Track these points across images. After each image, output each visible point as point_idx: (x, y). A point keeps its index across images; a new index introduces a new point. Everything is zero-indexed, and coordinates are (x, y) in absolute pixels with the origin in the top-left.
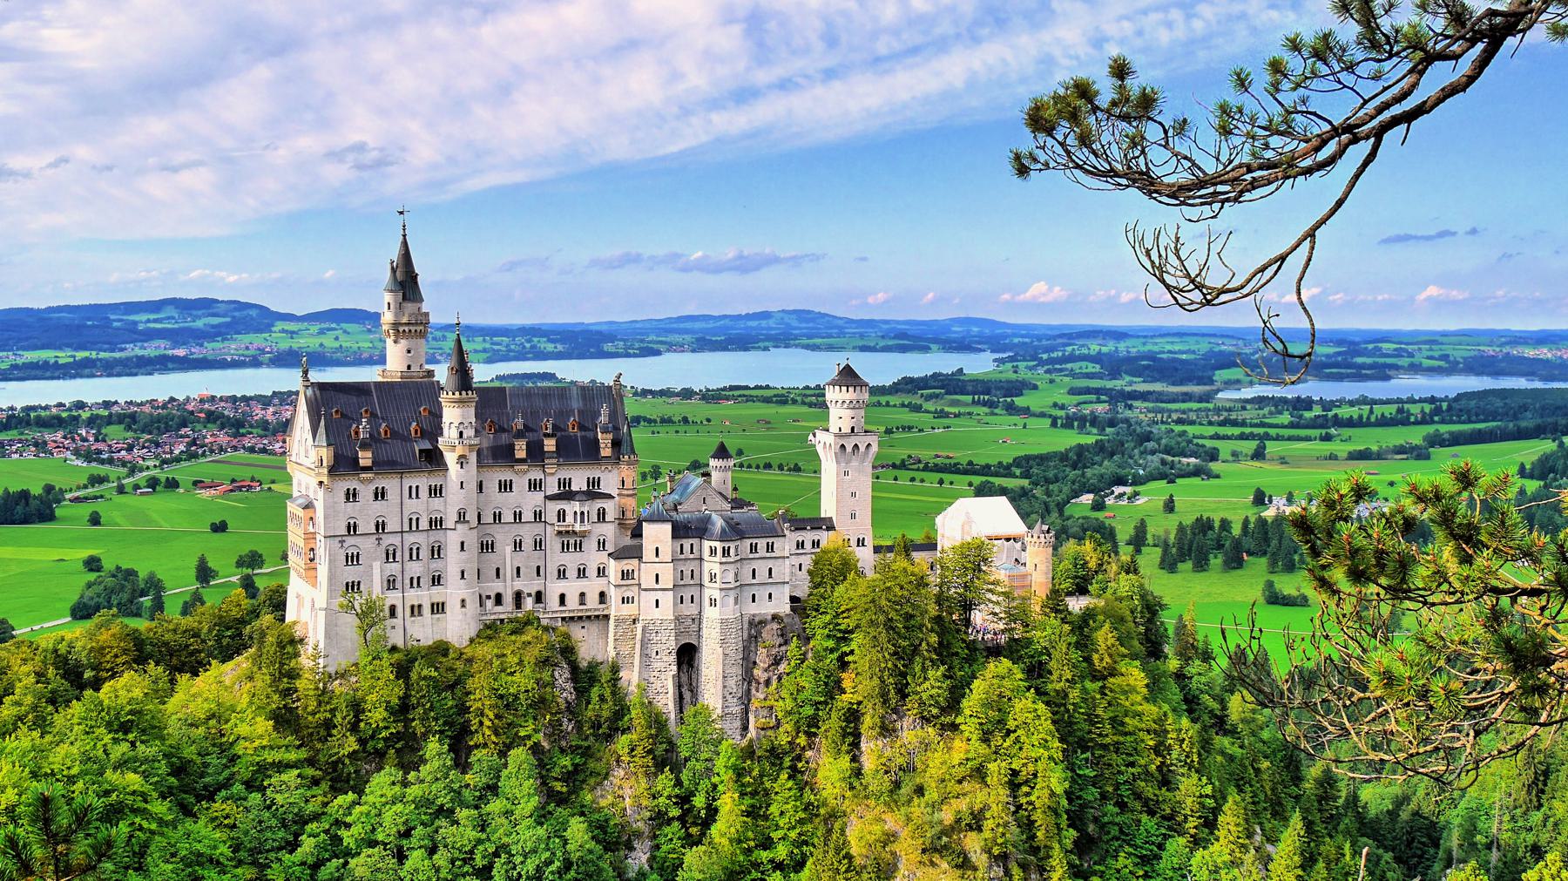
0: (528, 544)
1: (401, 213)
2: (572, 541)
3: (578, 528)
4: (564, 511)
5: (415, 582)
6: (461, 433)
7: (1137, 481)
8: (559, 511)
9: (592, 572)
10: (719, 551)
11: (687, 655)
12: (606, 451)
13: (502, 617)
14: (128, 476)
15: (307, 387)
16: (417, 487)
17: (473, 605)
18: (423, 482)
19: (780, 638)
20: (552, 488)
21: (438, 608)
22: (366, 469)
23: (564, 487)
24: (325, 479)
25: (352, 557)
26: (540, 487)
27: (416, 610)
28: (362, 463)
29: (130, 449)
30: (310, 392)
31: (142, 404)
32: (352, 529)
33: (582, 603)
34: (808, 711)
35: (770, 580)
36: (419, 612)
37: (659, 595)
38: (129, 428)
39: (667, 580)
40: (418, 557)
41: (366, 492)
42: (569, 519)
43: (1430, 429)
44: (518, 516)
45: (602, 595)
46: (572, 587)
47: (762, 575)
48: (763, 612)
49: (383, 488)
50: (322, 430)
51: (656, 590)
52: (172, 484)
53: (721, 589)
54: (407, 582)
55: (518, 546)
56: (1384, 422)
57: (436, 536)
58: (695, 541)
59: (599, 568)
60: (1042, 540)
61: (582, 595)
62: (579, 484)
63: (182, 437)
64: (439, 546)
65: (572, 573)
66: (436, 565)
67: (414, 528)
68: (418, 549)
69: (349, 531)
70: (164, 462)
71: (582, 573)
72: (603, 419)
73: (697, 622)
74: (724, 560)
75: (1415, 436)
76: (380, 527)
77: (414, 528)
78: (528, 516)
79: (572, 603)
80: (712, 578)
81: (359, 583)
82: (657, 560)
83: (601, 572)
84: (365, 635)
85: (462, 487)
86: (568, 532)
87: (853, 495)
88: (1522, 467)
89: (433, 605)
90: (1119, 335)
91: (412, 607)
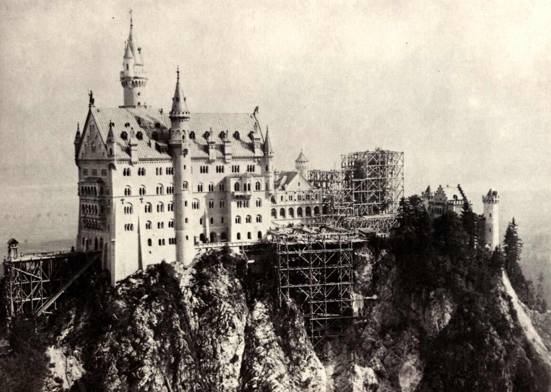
2: (243, 202)
8: (235, 184)
16: (161, 169)
17: (191, 239)
25: (128, 209)
27: (161, 242)
32: (128, 192)
41: (134, 170)
44: (211, 188)
49: (143, 169)
65: (243, 220)
68: (161, 206)
69: (126, 194)
76: (142, 191)
79: (244, 237)
89: (170, 239)
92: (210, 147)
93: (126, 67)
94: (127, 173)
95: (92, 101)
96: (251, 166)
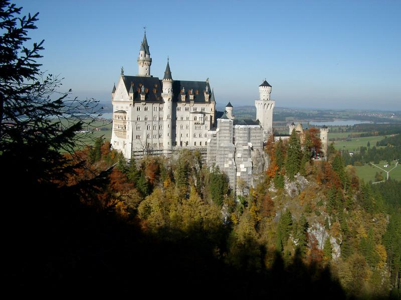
0: (184, 127)
1: (145, 28)
3: (200, 122)
5: (154, 137)
9: (203, 135)
12: (207, 100)
15: (123, 77)
18: (157, 105)
21: (161, 144)
22: (143, 101)
24: (132, 103)
28: (142, 99)
33: (200, 145)
41: (142, 109)
42: (198, 119)
43: (350, 134)
46: (198, 140)
50: (131, 89)
55: (181, 127)
56: (335, 132)
61: (201, 143)
62: (199, 110)
65: (197, 136)
75: (346, 135)
78: (185, 119)
79: (198, 144)
87: (267, 118)
88: (378, 143)
93: (141, 55)
94: (138, 109)
95: (123, 72)
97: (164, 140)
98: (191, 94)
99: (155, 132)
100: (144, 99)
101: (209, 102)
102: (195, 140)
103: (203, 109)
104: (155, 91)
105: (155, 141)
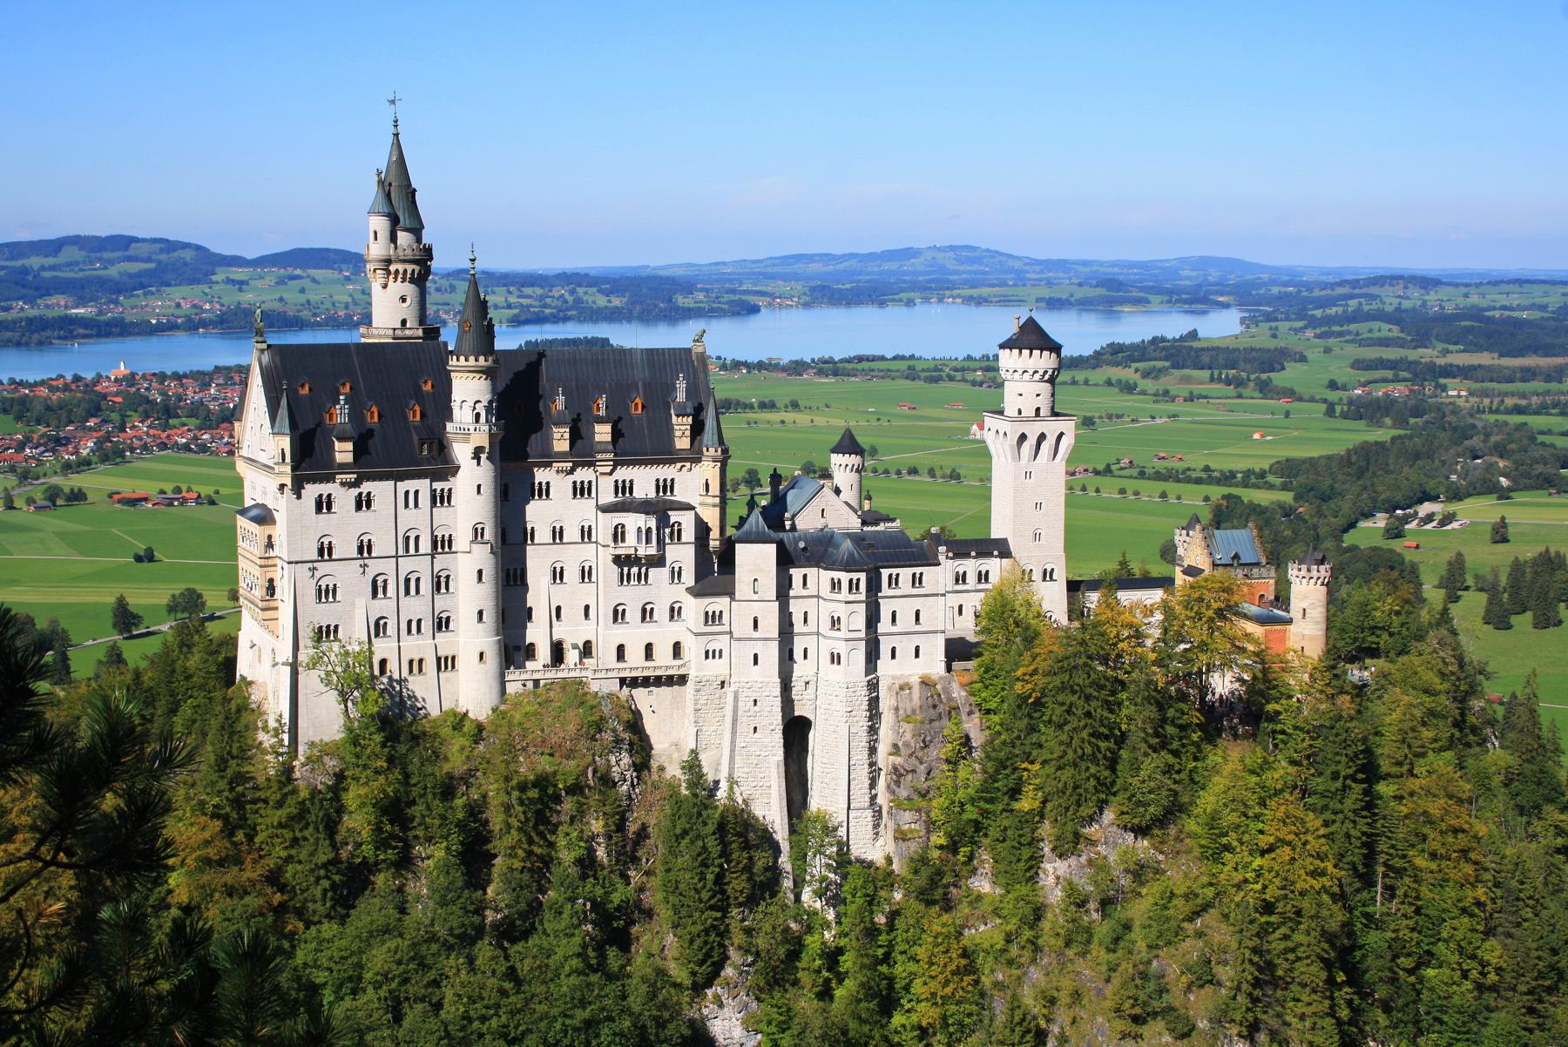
0: (572, 575)
3: (641, 552)
4: (623, 526)
6: (478, 415)
7: (1456, 495)
8: (616, 527)
9: (661, 613)
10: (845, 585)
11: (796, 731)
12: (682, 443)
13: (536, 676)
14: (19, 485)
16: (417, 492)
19: (932, 711)
20: (607, 496)
21: (446, 663)
23: (624, 493)
24: (288, 481)
26: (589, 494)
29: (21, 447)
30: (266, 358)
31: (36, 384)
32: (325, 551)
34: (971, 813)
35: (918, 628)
36: (420, 670)
37: (758, 648)
38: (19, 418)
39: (771, 626)
40: (418, 592)
41: (344, 498)
42: (631, 538)
44: (558, 534)
45: (677, 650)
46: (634, 635)
47: (906, 621)
48: (907, 673)
50: (283, 412)
51: (755, 639)
52: (77, 496)
53: (847, 640)
54: (404, 626)
55: (558, 575)
57: (441, 561)
58: (812, 572)
59: (672, 609)
60: (1314, 573)
61: (649, 649)
63: (90, 428)
64: (448, 577)
65: (633, 615)
66: (442, 602)
67: (412, 551)
70: (68, 467)
71: (646, 614)
72: (681, 396)
73: (812, 686)
74: (852, 598)
76: (364, 549)
77: (412, 551)
78: (572, 534)
79: (635, 656)
80: (835, 623)
81: (336, 627)
82: (755, 597)
83: (674, 613)
84: (345, 701)
85: (479, 492)
86: (628, 556)
87: (1038, 506)
89: (439, 659)
90: (1427, 283)
91: (411, 662)
92: (557, 436)
96: (665, 480)
97: (461, 640)
98: (601, 421)
99: (416, 607)
100: (349, 458)
101: (694, 457)
102: (619, 634)
103: (665, 486)
104: (415, 416)
105: (420, 646)
